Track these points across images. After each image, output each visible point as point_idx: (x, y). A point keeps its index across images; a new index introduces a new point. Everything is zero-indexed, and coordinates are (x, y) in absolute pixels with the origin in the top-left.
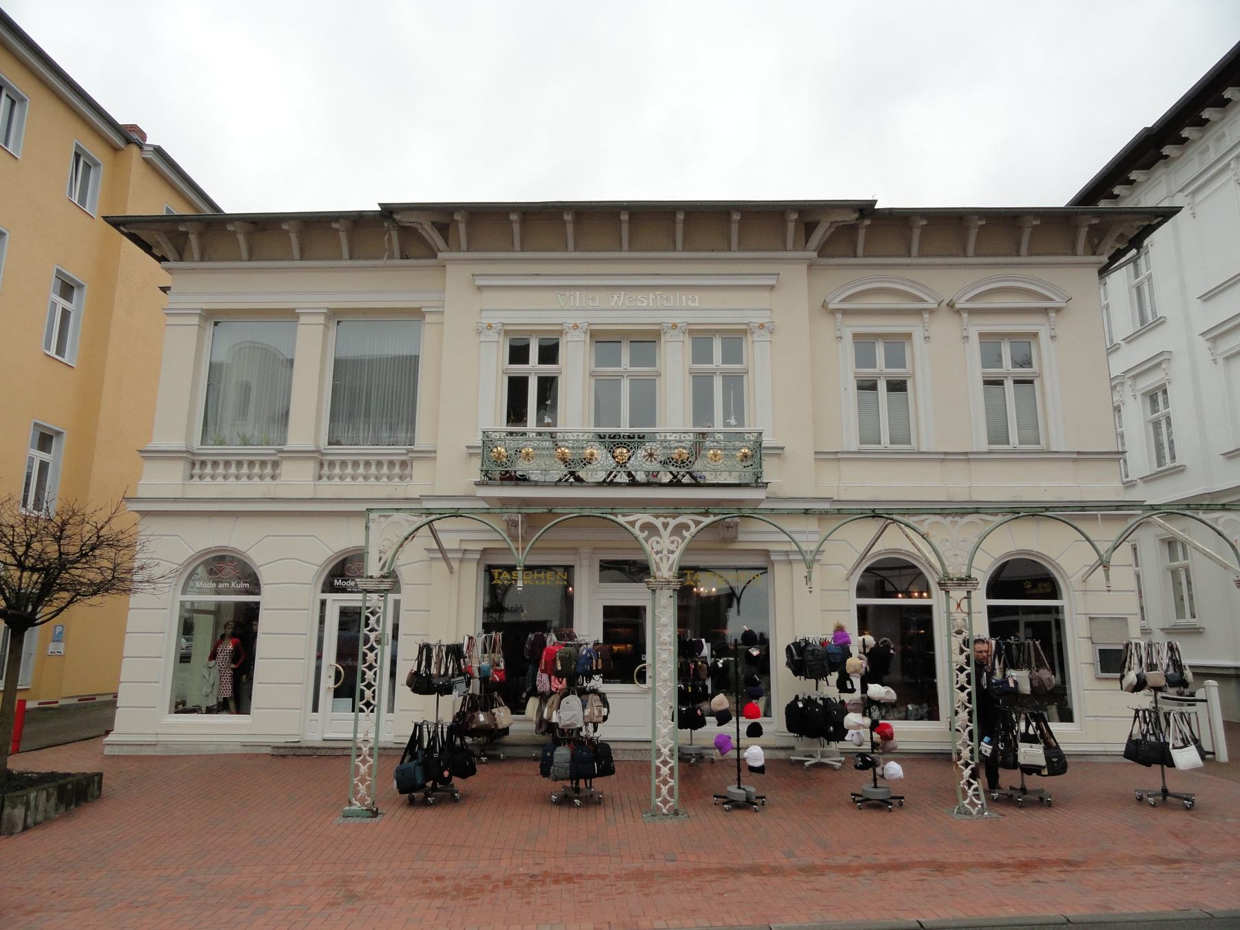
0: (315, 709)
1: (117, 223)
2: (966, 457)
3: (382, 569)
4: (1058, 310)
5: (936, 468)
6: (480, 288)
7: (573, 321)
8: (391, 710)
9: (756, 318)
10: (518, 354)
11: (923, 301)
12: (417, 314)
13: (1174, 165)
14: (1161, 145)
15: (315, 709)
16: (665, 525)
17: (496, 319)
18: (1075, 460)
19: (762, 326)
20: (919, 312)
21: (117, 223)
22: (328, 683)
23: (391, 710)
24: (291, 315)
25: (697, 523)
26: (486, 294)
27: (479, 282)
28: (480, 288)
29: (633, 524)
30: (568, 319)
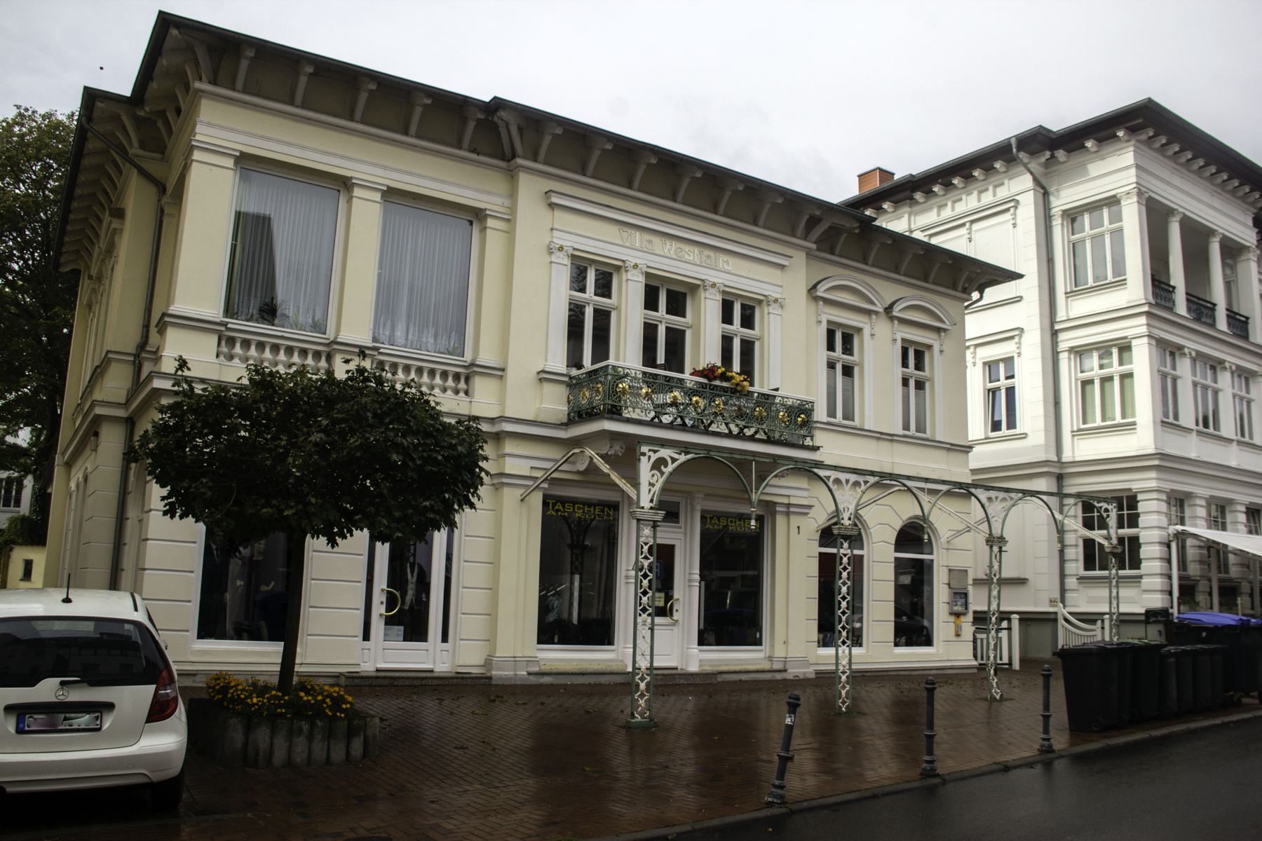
0: (366, 637)
1: (1020, 276)
2: (890, 438)
3: (652, 501)
4: (945, 330)
5: (872, 444)
6: (552, 206)
7: (634, 261)
8: (445, 638)
9: (773, 293)
10: (578, 282)
11: (942, 321)
12: (476, 216)
13: (916, 208)
14: (914, 190)
15: (366, 637)
16: (847, 481)
17: (569, 242)
18: (948, 449)
19: (776, 301)
20: (869, 313)
21: (1020, 276)
22: (379, 609)
23: (445, 638)
24: (344, 184)
25: (866, 482)
26: (558, 214)
27: (555, 199)
28: (552, 206)
29: (828, 478)
30: (632, 257)
